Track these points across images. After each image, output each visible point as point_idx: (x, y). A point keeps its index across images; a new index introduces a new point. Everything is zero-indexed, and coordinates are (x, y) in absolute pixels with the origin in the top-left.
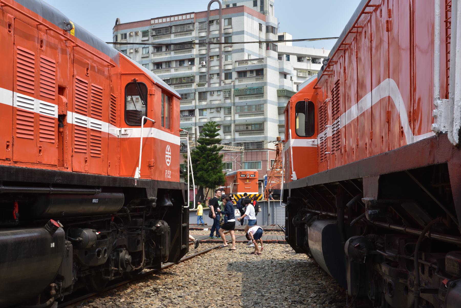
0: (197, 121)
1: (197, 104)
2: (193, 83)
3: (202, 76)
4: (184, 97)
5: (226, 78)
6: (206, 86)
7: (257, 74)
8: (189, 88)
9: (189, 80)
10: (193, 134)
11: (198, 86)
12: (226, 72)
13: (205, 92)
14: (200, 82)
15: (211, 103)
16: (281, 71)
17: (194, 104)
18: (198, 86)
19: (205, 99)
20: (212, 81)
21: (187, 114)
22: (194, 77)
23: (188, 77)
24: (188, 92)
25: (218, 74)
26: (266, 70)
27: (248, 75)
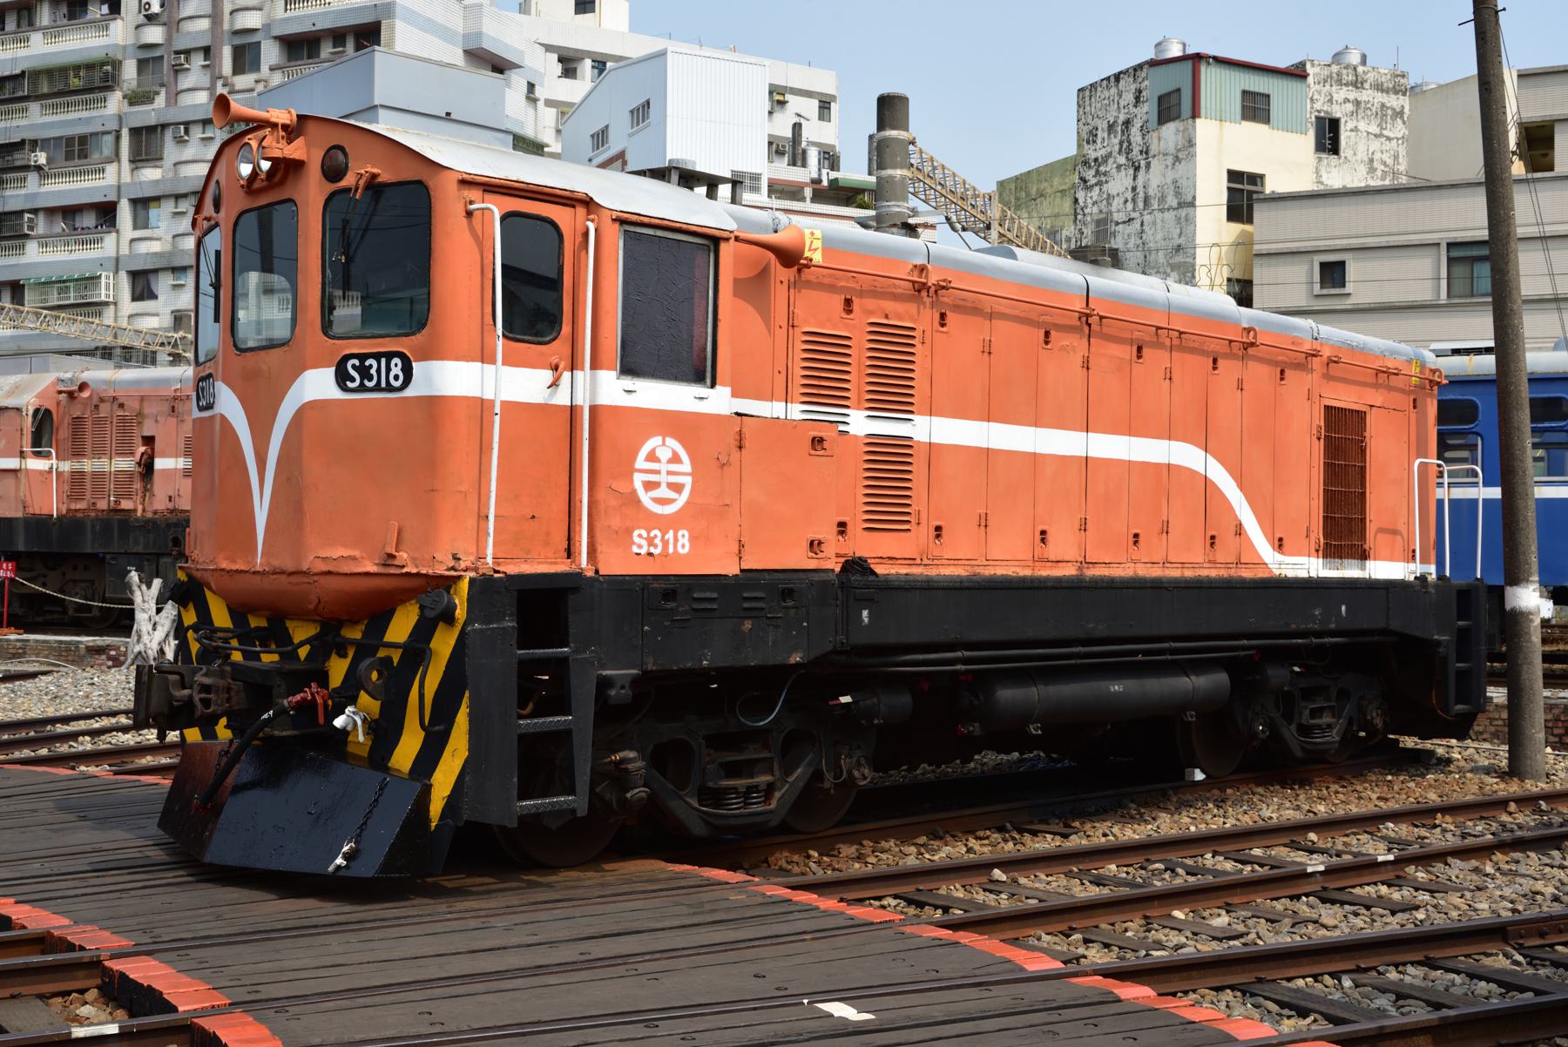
0: (125, 250)
1: (126, 177)
2: (110, 88)
3: (148, 59)
4: (77, 149)
5: (238, 69)
6: (160, 101)
7: (359, 47)
8: (94, 113)
9: (96, 78)
10: (106, 304)
11: (131, 104)
12: (238, 41)
13: (151, 129)
14: (139, 85)
15: (176, 172)
16: (472, 46)
17: (112, 178)
18: (131, 104)
19: (155, 158)
20: (186, 81)
21: (89, 220)
22: (117, 65)
23: (90, 67)
24: (91, 129)
25: (207, 51)
26: (392, 28)
27: (326, 50)
